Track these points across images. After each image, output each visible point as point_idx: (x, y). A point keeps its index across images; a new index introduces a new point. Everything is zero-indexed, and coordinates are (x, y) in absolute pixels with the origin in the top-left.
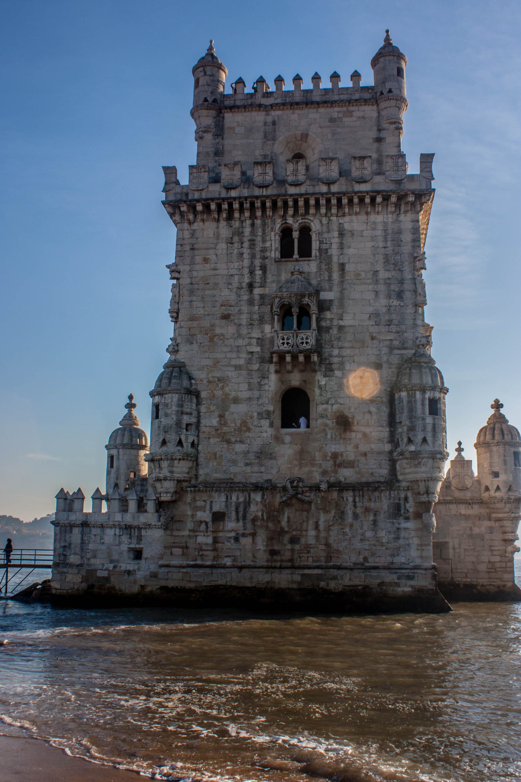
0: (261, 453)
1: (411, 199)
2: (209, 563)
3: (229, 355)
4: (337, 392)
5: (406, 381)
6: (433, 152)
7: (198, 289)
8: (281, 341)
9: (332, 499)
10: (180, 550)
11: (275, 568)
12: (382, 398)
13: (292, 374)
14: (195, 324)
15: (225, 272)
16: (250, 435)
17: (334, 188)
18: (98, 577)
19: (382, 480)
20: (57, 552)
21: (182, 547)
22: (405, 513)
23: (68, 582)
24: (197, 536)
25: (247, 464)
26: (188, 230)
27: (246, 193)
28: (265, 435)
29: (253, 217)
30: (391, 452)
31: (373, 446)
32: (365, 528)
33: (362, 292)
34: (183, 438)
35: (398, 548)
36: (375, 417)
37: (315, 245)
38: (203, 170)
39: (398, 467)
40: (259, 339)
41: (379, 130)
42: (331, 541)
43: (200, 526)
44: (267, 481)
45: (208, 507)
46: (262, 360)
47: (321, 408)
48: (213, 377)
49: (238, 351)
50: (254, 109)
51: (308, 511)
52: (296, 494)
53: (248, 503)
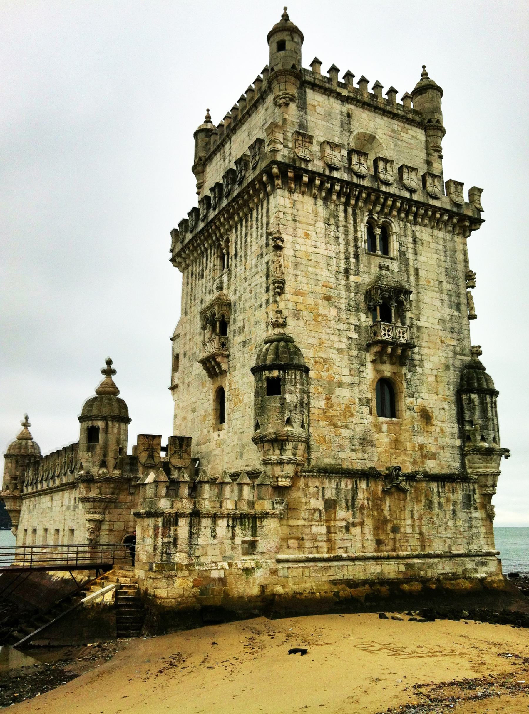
0: (364, 439)
1: (467, 224)
2: (326, 556)
3: (332, 337)
7: (301, 264)
9: (422, 489)
11: (384, 558)
14: (300, 299)
15: (325, 252)
17: (415, 197)
19: (456, 472)
25: (353, 450)
27: (345, 177)
28: (365, 421)
30: (461, 448)
31: (448, 440)
32: (448, 517)
36: (448, 413)
38: (308, 140)
39: (467, 462)
40: (356, 326)
42: (424, 531)
43: (313, 514)
45: (320, 494)
47: (409, 400)
48: (319, 357)
51: (405, 500)
53: (355, 491)
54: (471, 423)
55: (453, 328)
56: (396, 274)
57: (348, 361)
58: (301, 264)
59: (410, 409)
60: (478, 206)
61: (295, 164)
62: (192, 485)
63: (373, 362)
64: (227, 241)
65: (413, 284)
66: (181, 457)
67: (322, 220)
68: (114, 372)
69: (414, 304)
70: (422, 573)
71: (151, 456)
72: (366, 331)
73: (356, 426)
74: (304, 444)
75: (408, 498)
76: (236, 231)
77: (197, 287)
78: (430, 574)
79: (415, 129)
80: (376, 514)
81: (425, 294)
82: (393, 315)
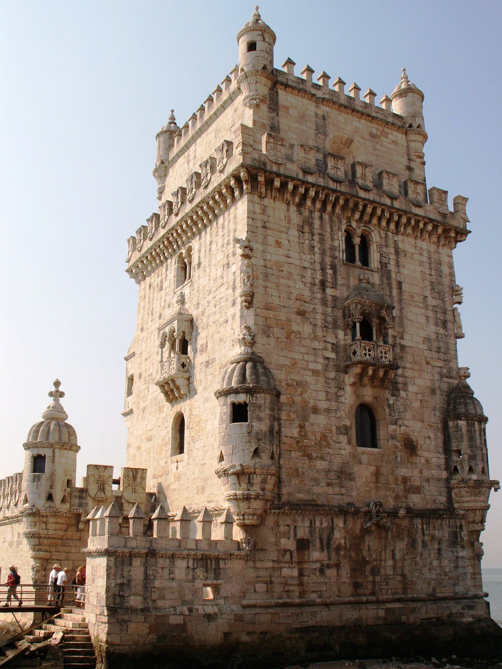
0: (341, 472)
1: (453, 235)
2: (297, 601)
3: (306, 357)
4: (403, 414)
5: (464, 410)
6: (467, 197)
7: (272, 275)
8: (364, 352)
9: (406, 527)
10: (265, 585)
12: (437, 423)
13: (365, 388)
14: (271, 314)
15: (298, 262)
16: (330, 451)
17: (396, 204)
18: (170, 625)
19: (442, 507)
20: (112, 592)
21: (266, 583)
22: (461, 541)
23: (130, 635)
24: (282, 568)
25: (329, 485)
26: (258, 203)
27: (321, 182)
28: (343, 452)
29: (323, 209)
30: (448, 480)
31: (433, 472)
32: (432, 557)
33: (417, 314)
34: (275, 450)
35: (458, 578)
36: (433, 443)
37: (375, 257)
38: (280, 143)
40: (333, 344)
41: (410, 160)
42: (406, 572)
43: (284, 555)
44: (348, 504)
45: (292, 533)
46: (338, 370)
47: (392, 428)
48: (292, 380)
49: (315, 354)
50: (306, 96)
51: (386, 538)
52: (378, 519)
53: (332, 529)
54: (459, 452)
55: (439, 348)
56: (377, 287)
57: (324, 384)
58: (272, 275)
59: (393, 437)
60: (463, 216)
61: (266, 167)
62: (147, 522)
63: (353, 384)
64: (190, 250)
65: (396, 299)
66: (135, 491)
67: (295, 227)
68: (62, 394)
69: (397, 320)
70: (404, 618)
71: (102, 488)
72: (345, 350)
73: (333, 457)
74: (274, 478)
75: (389, 536)
76: (200, 238)
77: (155, 301)
78: (412, 618)
79: (395, 133)
80: (353, 554)
81: (408, 310)
82: (374, 332)
